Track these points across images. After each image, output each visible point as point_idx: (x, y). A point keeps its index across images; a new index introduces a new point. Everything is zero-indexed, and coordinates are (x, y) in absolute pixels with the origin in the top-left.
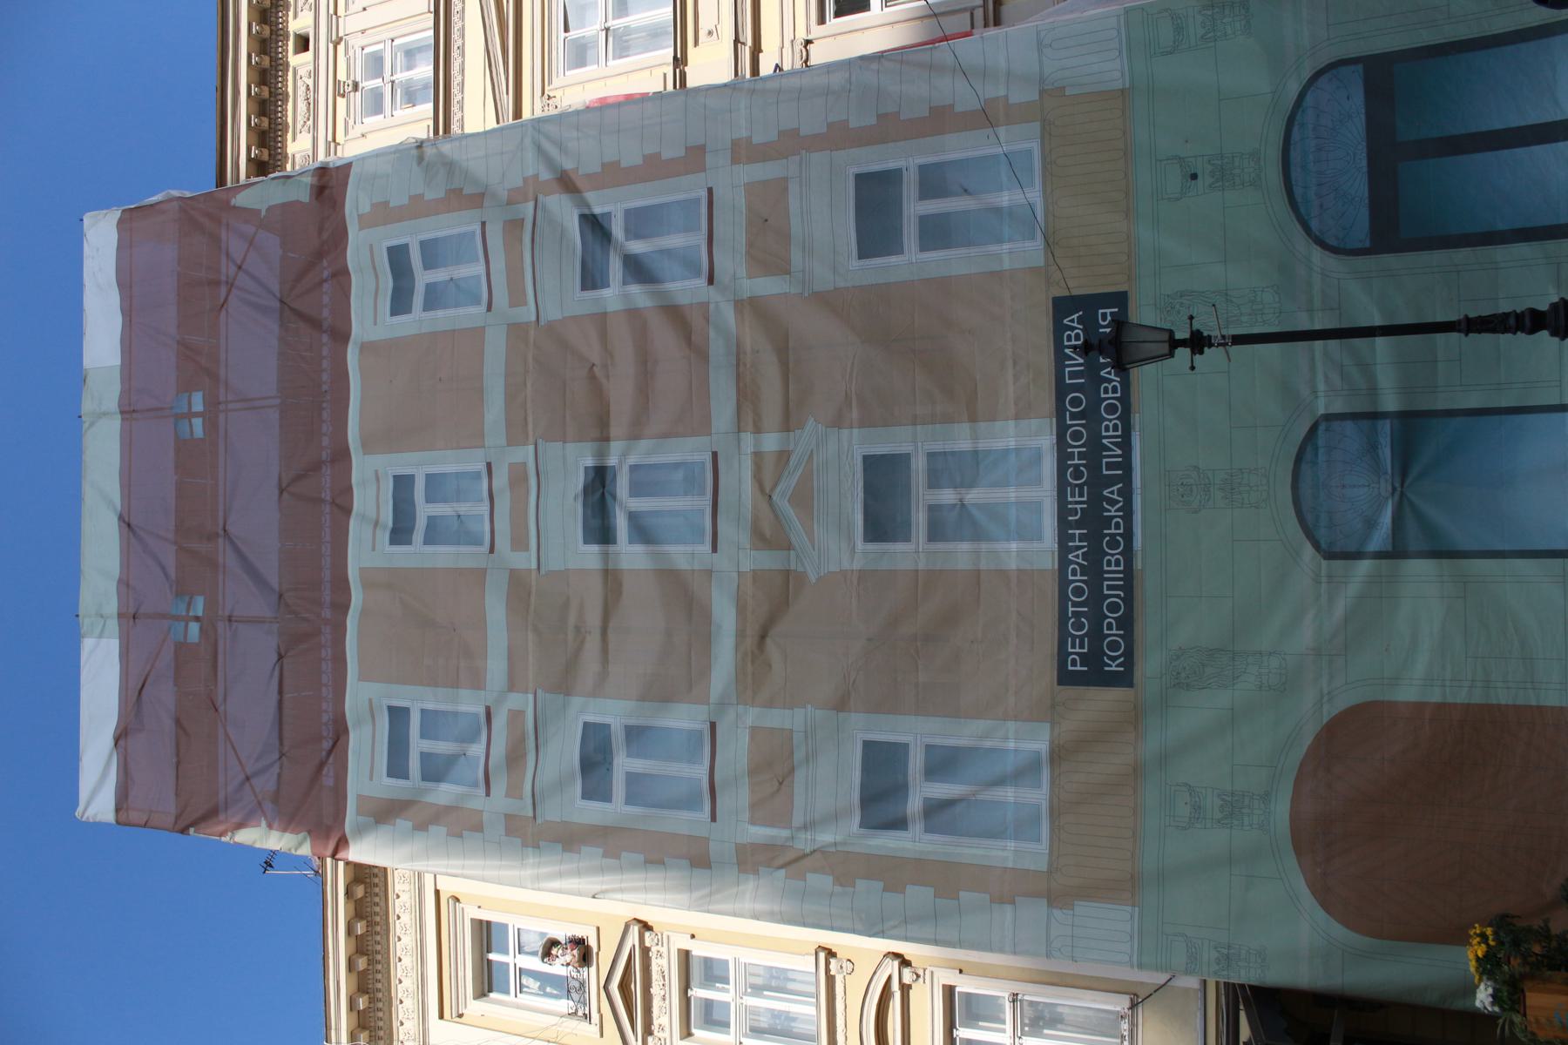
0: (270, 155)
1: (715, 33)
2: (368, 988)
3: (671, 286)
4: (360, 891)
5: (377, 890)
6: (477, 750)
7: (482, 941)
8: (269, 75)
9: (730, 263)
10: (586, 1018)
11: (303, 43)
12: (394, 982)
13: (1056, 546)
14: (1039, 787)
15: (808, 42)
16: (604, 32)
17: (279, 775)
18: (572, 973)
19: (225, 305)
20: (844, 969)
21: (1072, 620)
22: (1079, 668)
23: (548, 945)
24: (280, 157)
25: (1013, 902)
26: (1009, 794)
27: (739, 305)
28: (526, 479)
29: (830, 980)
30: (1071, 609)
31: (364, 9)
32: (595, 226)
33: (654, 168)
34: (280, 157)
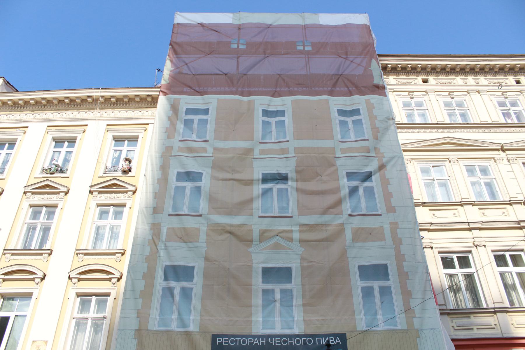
0: (389, 71)
1: (434, 216)
2: (118, 102)
3: (348, 201)
4: (149, 99)
5: (149, 105)
6: (194, 138)
7: (132, 138)
8: (414, 70)
9: (356, 222)
10: (105, 172)
11: (425, 81)
12: (119, 110)
13: (260, 334)
14: (177, 327)
15: (432, 248)
16: (433, 179)
17: (188, 74)
18: (120, 168)
19: (339, 57)
20: (118, 259)
21: (234, 340)
22: (218, 341)
23: (129, 160)
24: (388, 74)
25: (137, 317)
26: (175, 316)
27: (342, 225)
28: (283, 154)
29: (114, 254)
30: (238, 339)
31: (437, 101)
32: (368, 177)
33: (388, 196)
34: (388, 74)
